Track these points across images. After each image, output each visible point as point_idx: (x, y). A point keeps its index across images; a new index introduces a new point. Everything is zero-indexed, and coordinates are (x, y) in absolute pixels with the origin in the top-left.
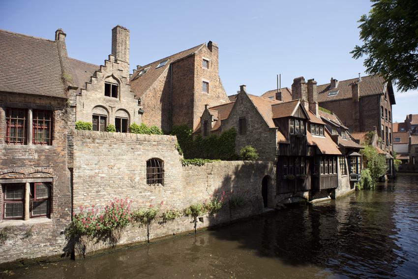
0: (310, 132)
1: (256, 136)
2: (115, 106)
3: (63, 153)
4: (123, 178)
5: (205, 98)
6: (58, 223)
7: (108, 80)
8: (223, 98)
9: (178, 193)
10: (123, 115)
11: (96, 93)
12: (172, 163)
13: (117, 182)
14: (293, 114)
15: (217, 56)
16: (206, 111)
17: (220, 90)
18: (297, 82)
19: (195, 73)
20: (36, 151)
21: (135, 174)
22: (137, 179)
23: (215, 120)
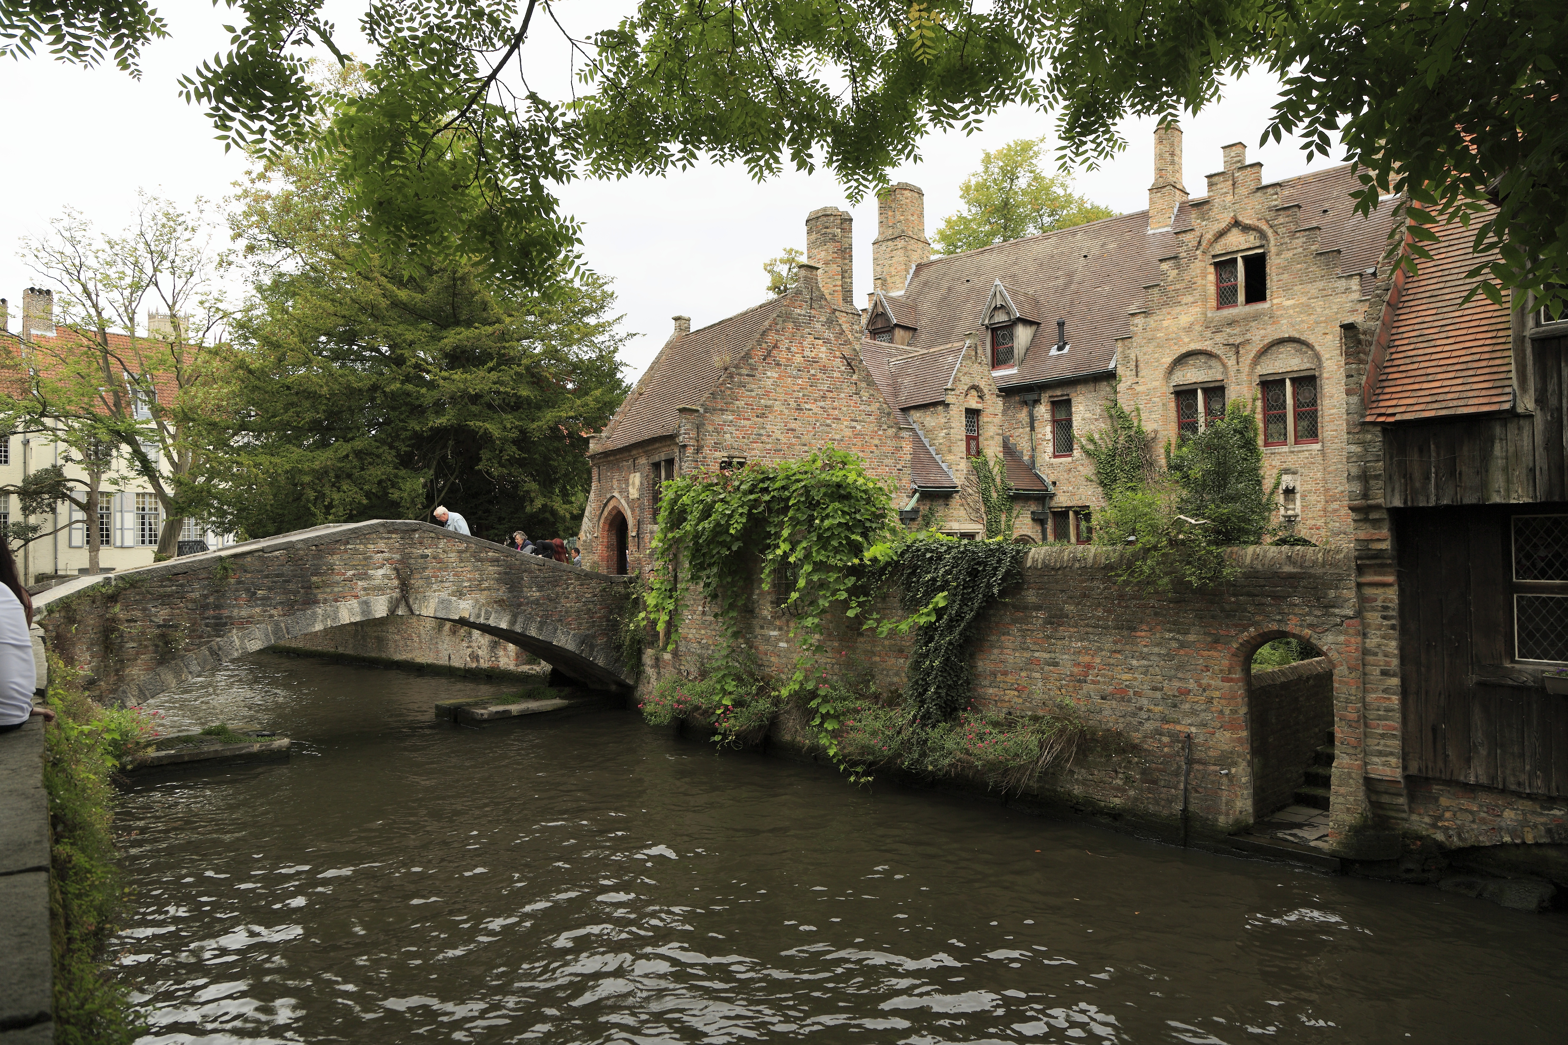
2: (1248, 336)
7: (1219, 248)
10: (1288, 362)
11: (1178, 309)
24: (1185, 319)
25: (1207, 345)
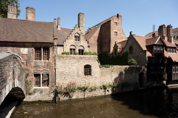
0: (167, 51)
1: (137, 54)
3: (52, 63)
4: (74, 73)
5: (116, 39)
6: (51, 89)
7: (75, 35)
8: (124, 38)
9: (98, 79)
10: (81, 48)
12: (95, 66)
13: (72, 74)
14: (156, 43)
15: (121, 20)
16: (116, 44)
17: (123, 35)
18: (161, 28)
19: (111, 28)
20: (44, 63)
21: (79, 71)
22: (80, 73)
23: (119, 48)
24: (72, 41)
25: (74, 45)
